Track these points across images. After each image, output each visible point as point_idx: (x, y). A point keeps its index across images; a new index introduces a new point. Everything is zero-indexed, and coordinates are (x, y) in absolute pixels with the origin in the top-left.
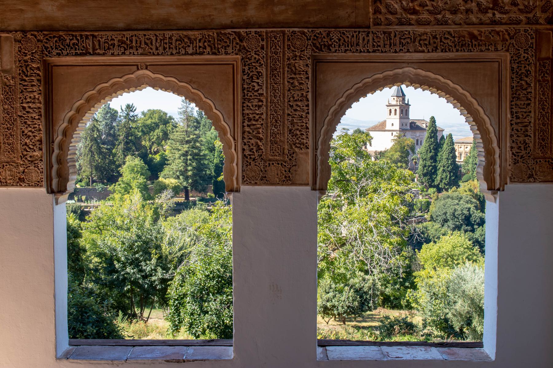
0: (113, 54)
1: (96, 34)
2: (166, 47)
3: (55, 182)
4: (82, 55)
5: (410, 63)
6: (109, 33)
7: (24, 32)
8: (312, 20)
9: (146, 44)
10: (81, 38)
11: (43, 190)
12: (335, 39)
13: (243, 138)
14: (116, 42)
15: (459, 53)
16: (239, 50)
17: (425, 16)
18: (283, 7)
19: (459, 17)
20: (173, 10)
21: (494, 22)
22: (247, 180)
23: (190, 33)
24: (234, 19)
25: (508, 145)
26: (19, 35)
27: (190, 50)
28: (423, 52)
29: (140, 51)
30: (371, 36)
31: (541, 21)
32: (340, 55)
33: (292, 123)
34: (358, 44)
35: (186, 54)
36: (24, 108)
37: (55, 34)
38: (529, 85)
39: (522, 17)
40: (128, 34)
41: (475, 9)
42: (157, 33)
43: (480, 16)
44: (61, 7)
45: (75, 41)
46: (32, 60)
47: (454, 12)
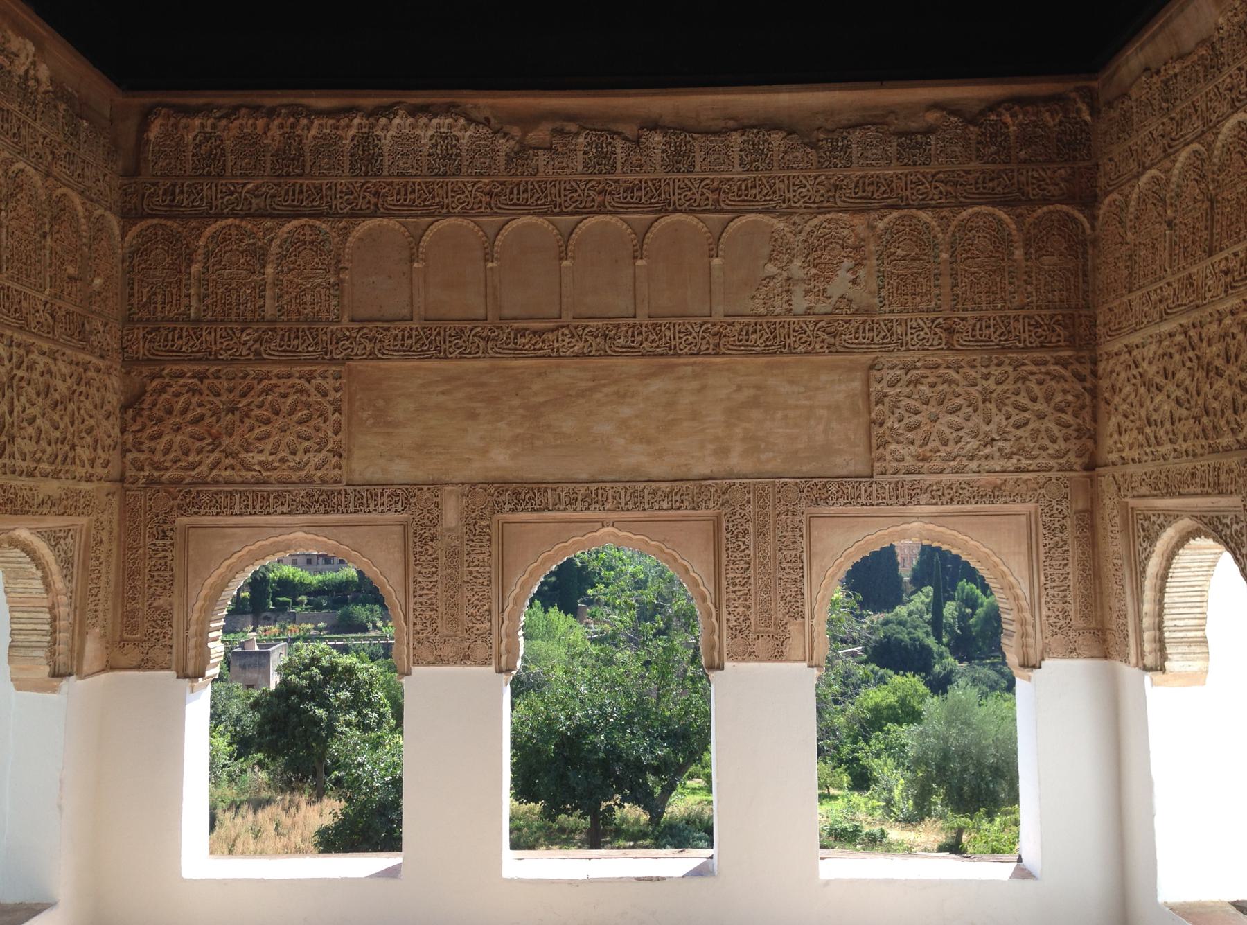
0: (575, 510)
1: (555, 486)
2: (638, 501)
3: (504, 658)
4: (537, 510)
5: (919, 517)
6: (571, 486)
7: (474, 485)
8: (804, 469)
9: (614, 498)
10: (539, 490)
11: (492, 669)
12: (833, 490)
13: (728, 606)
14: (580, 498)
15: (978, 506)
16: (722, 505)
17: (937, 463)
18: (771, 454)
19: (974, 465)
20: (644, 459)
21: (1019, 470)
22: (734, 657)
23: (663, 485)
24: (715, 469)
25: (1045, 612)
26: (468, 488)
27: (665, 506)
28: (936, 504)
29: (607, 507)
30: (874, 486)
31: (1076, 467)
32: (837, 509)
33: (785, 589)
34: (859, 497)
35: (661, 509)
36: (471, 573)
37: (506, 486)
38: (1065, 543)
39: (1053, 463)
40: (593, 487)
41: (997, 455)
42: (627, 485)
43: (1003, 462)
44: (514, 457)
45: (531, 495)
46: (481, 517)
47: (972, 458)
